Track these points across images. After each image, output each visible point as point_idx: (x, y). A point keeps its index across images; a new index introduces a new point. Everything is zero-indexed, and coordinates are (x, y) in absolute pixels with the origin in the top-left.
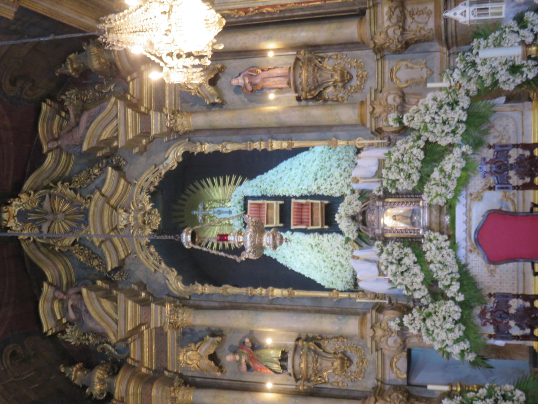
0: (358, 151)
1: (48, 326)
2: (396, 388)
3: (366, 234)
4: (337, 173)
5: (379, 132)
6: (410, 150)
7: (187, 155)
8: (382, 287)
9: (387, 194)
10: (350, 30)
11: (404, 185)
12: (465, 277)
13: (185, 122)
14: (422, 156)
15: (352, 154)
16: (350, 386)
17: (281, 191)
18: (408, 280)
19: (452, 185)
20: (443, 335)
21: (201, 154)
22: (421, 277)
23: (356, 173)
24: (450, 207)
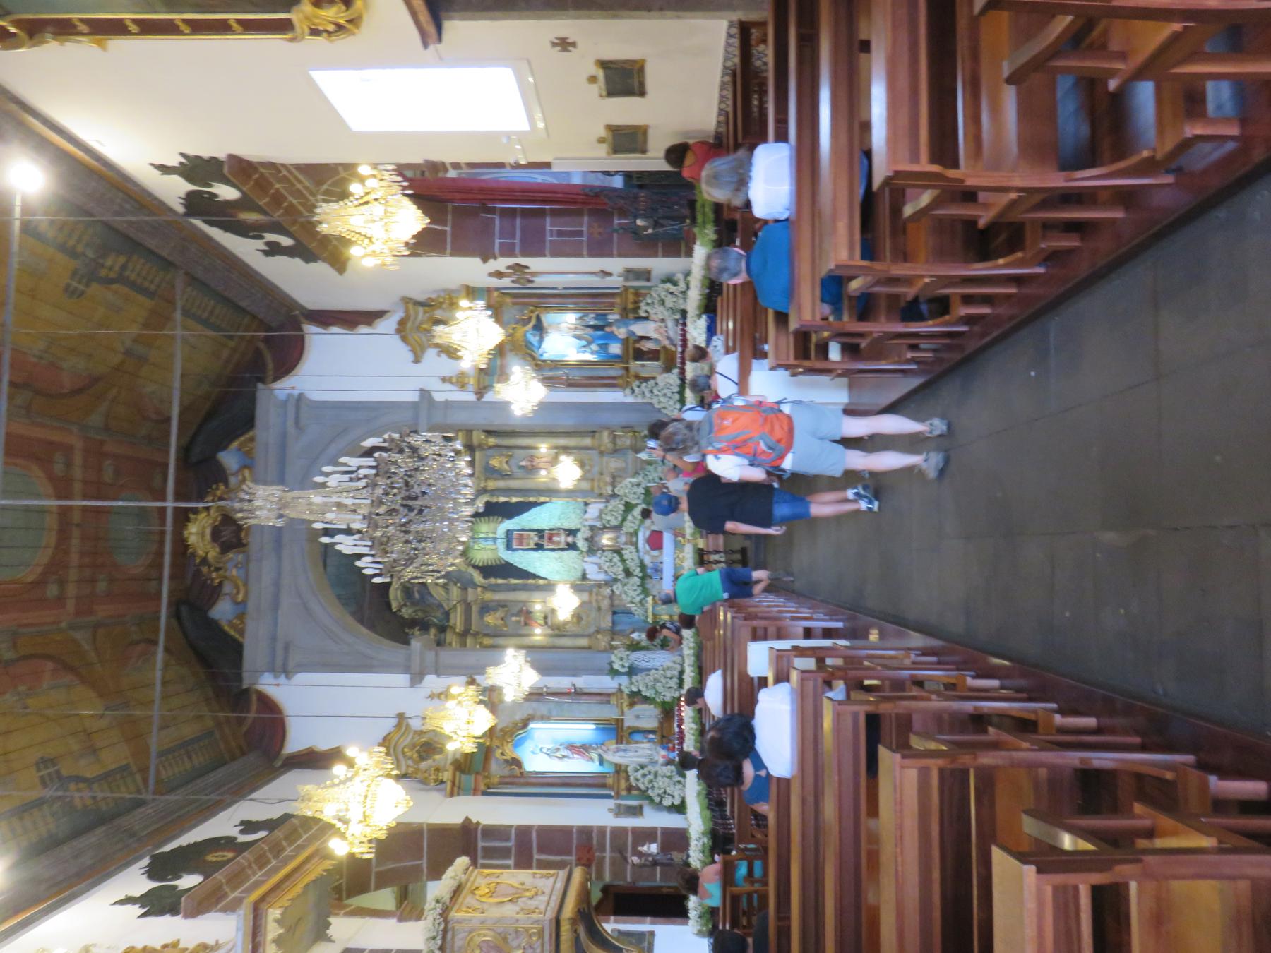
0: (586, 504)
1: (394, 606)
2: (605, 630)
3: (593, 548)
4: (573, 516)
5: (601, 495)
6: (617, 505)
7: (488, 504)
8: (601, 577)
9: (605, 527)
10: (587, 441)
11: (614, 522)
12: (643, 566)
13: (491, 484)
14: (623, 508)
15: (582, 505)
16: (581, 632)
17: (535, 527)
18: (615, 570)
19: (637, 522)
20: (631, 593)
21: (497, 503)
22: (621, 568)
23: (587, 516)
24: (636, 533)
